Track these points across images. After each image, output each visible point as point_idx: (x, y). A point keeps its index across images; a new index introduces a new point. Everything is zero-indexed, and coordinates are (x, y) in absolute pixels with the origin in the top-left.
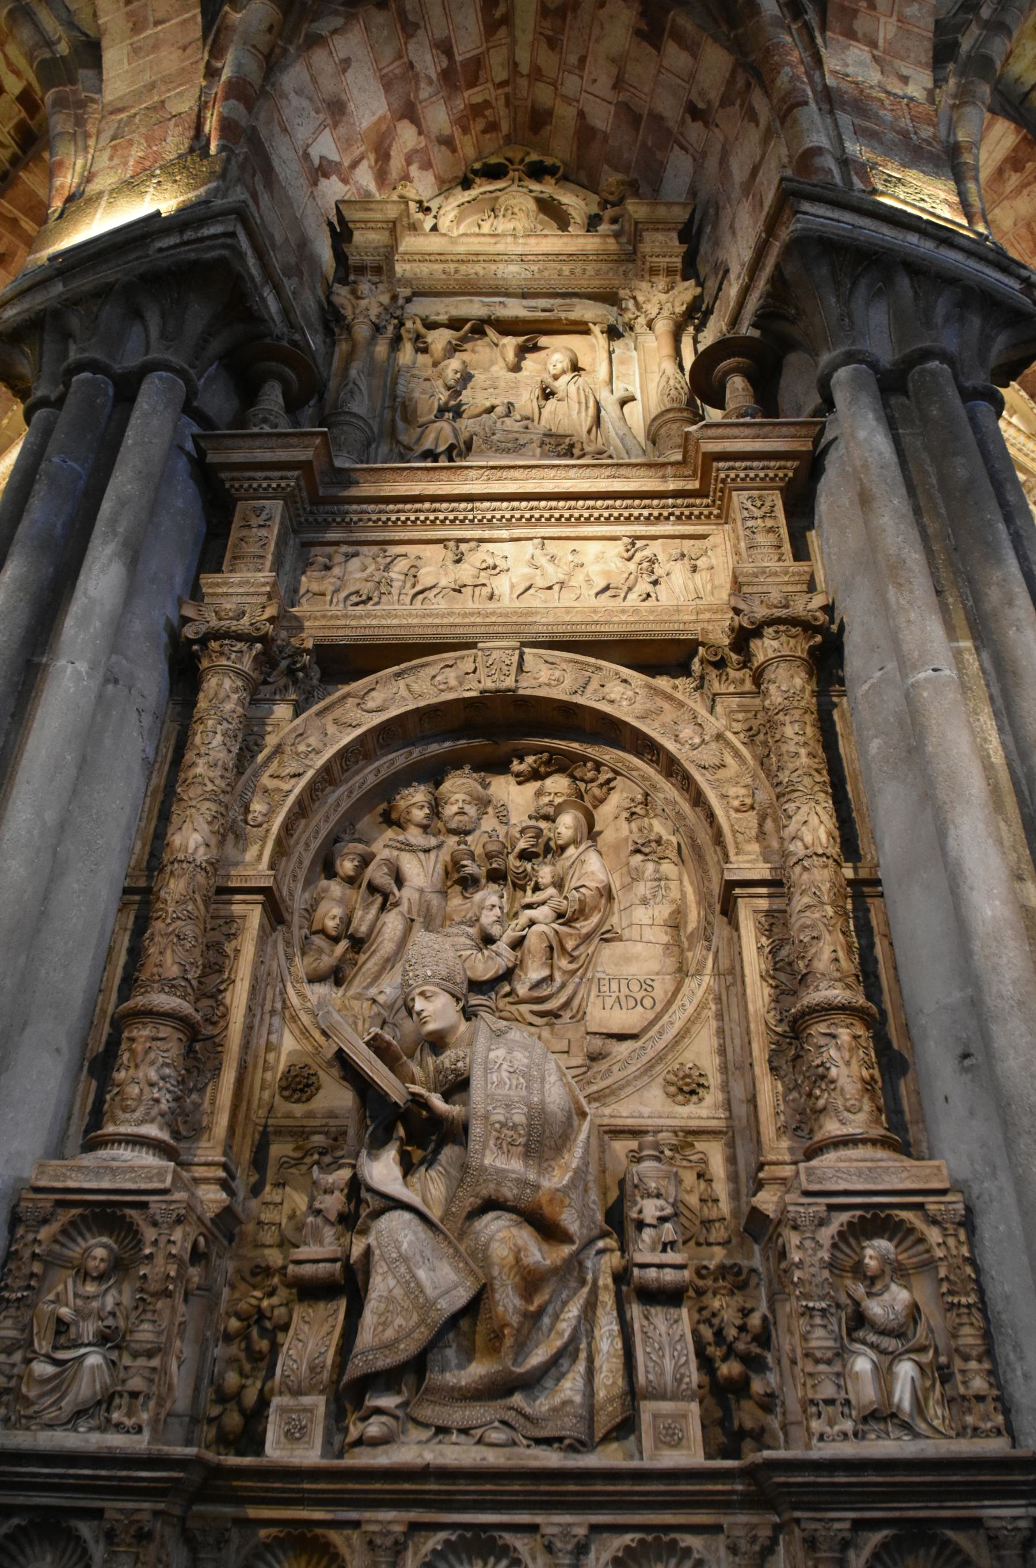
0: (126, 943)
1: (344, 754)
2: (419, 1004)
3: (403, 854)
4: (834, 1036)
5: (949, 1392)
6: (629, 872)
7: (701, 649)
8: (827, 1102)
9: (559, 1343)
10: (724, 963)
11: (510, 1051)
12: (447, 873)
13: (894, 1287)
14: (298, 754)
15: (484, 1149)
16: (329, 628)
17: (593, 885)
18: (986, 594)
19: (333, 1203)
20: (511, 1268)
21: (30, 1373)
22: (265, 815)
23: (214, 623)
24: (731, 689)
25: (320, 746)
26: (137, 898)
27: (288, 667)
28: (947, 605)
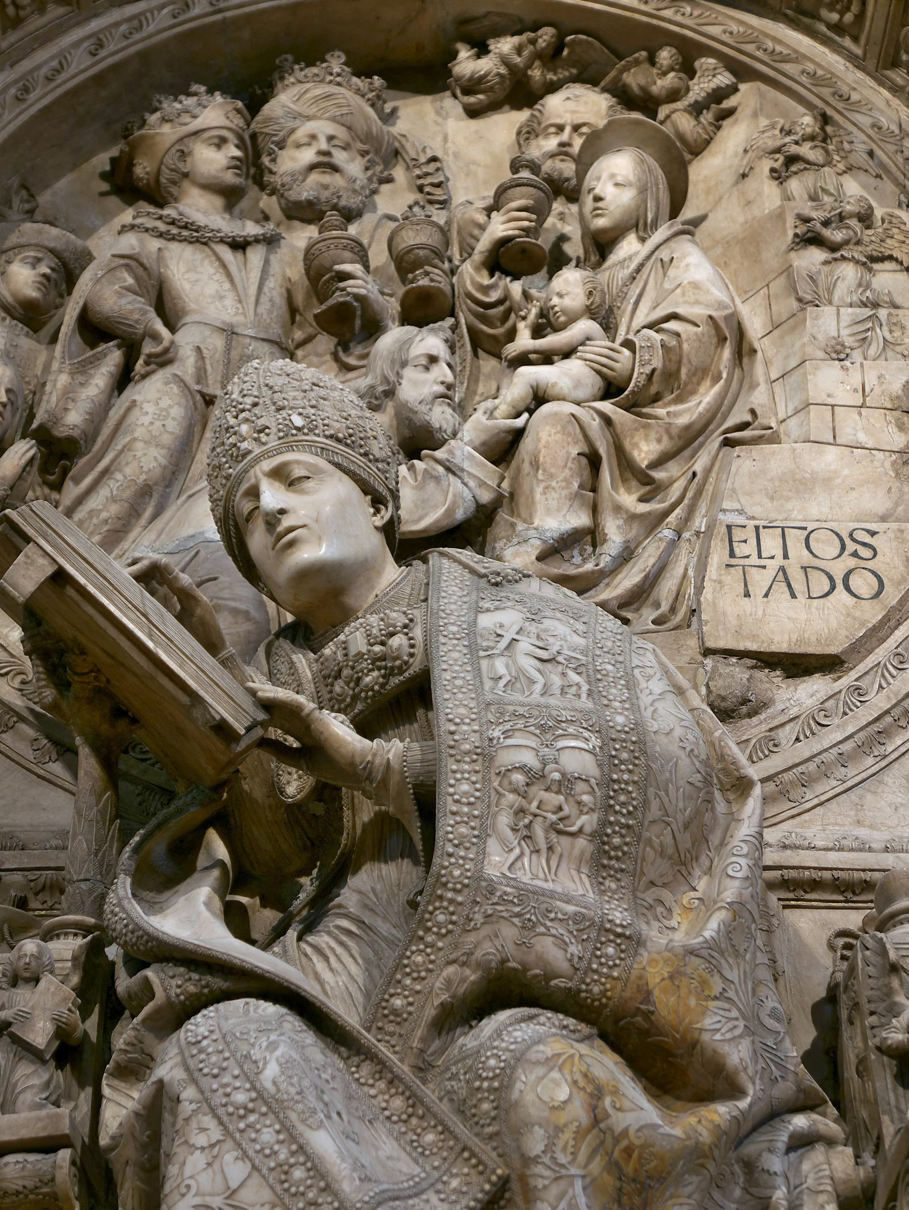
3: (174, 246)
6: (792, 287)
11: (534, 617)
12: (293, 311)
15: (482, 838)
20: (580, 1135)
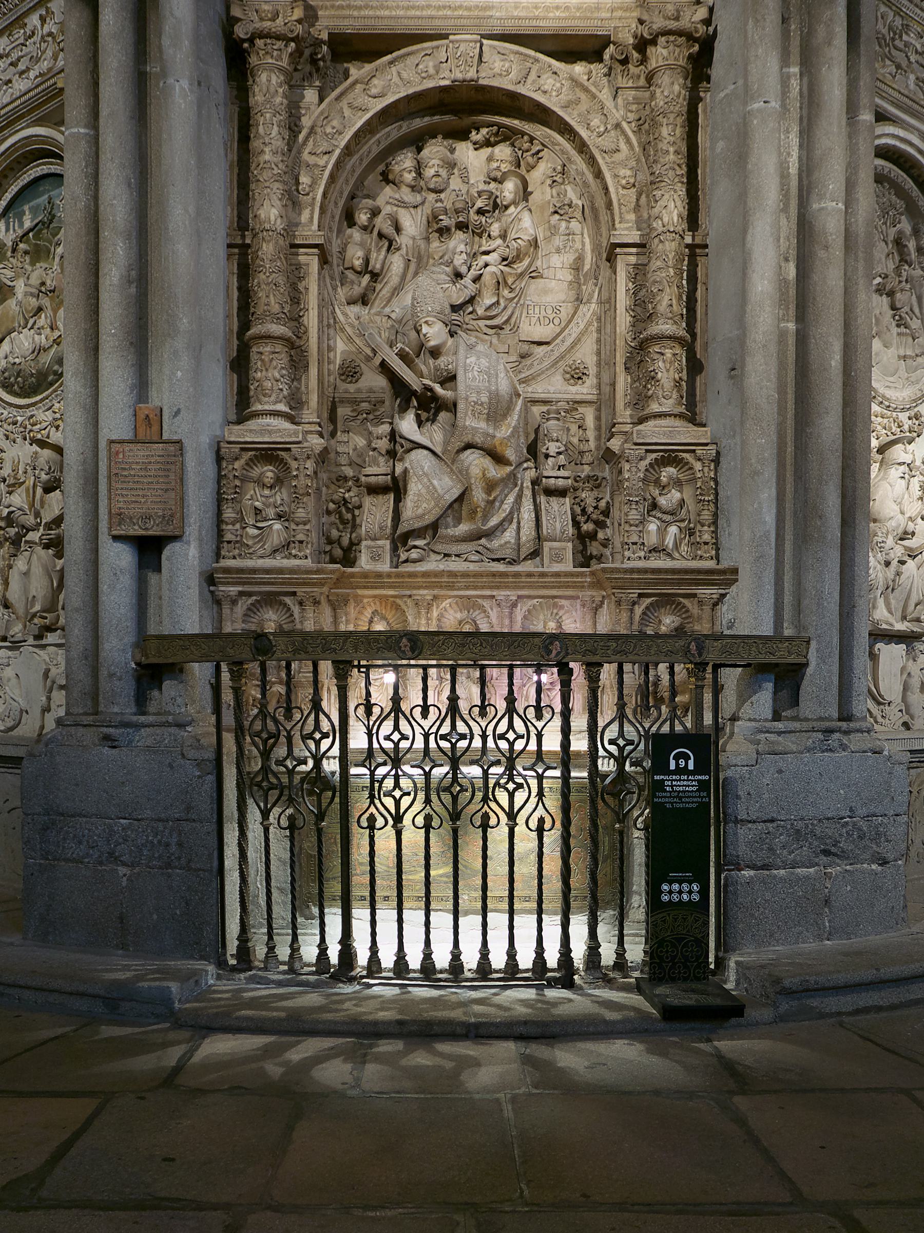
0: (236, 284)
1: (357, 135)
2: (425, 329)
4: (663, 354)
5: (692, 540)
6: (550, 229)
7: (611, 45)
8: (654, 392)
9: (504, 515)
10: (605, 295)
12: (429, 223)
13: (673, 491)
14: (327, 135)
16: (338, 17)
17: (526, 238)
18: (816, 31)
19: (383, 444)
21: (247, 533)
22: (310, 186)
23: (258, 25)
24: (630, 84)
25: (340, 127)
26: (236, 250)
27: (311, 55)
28: (789, 31)
